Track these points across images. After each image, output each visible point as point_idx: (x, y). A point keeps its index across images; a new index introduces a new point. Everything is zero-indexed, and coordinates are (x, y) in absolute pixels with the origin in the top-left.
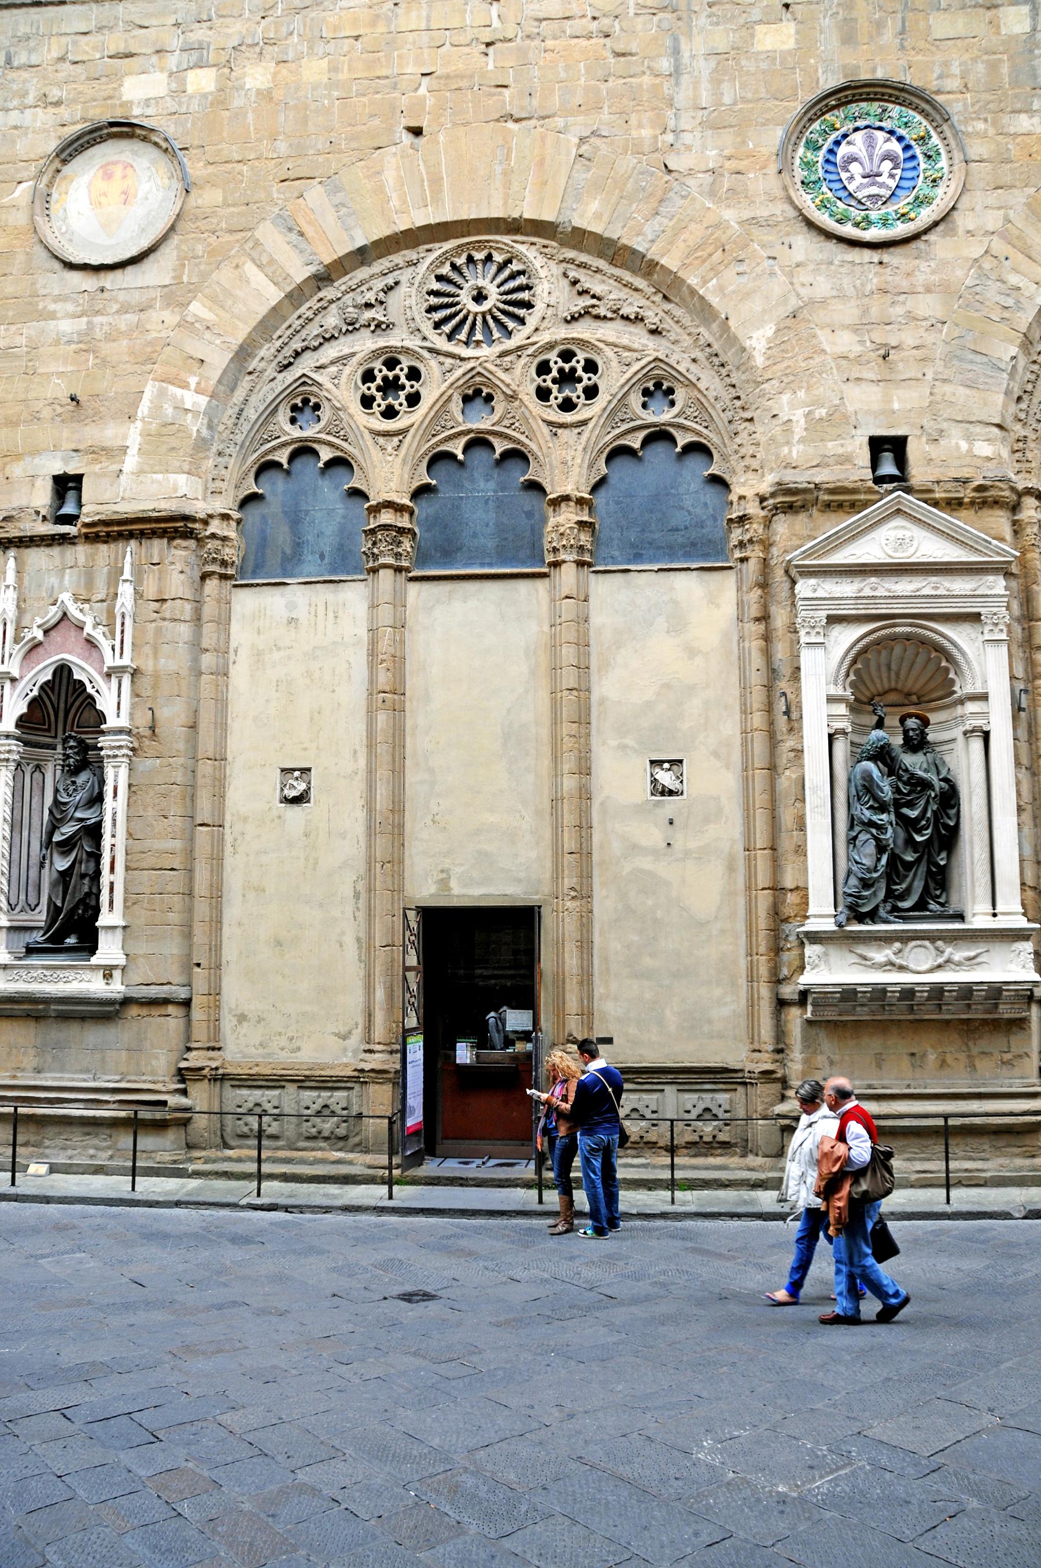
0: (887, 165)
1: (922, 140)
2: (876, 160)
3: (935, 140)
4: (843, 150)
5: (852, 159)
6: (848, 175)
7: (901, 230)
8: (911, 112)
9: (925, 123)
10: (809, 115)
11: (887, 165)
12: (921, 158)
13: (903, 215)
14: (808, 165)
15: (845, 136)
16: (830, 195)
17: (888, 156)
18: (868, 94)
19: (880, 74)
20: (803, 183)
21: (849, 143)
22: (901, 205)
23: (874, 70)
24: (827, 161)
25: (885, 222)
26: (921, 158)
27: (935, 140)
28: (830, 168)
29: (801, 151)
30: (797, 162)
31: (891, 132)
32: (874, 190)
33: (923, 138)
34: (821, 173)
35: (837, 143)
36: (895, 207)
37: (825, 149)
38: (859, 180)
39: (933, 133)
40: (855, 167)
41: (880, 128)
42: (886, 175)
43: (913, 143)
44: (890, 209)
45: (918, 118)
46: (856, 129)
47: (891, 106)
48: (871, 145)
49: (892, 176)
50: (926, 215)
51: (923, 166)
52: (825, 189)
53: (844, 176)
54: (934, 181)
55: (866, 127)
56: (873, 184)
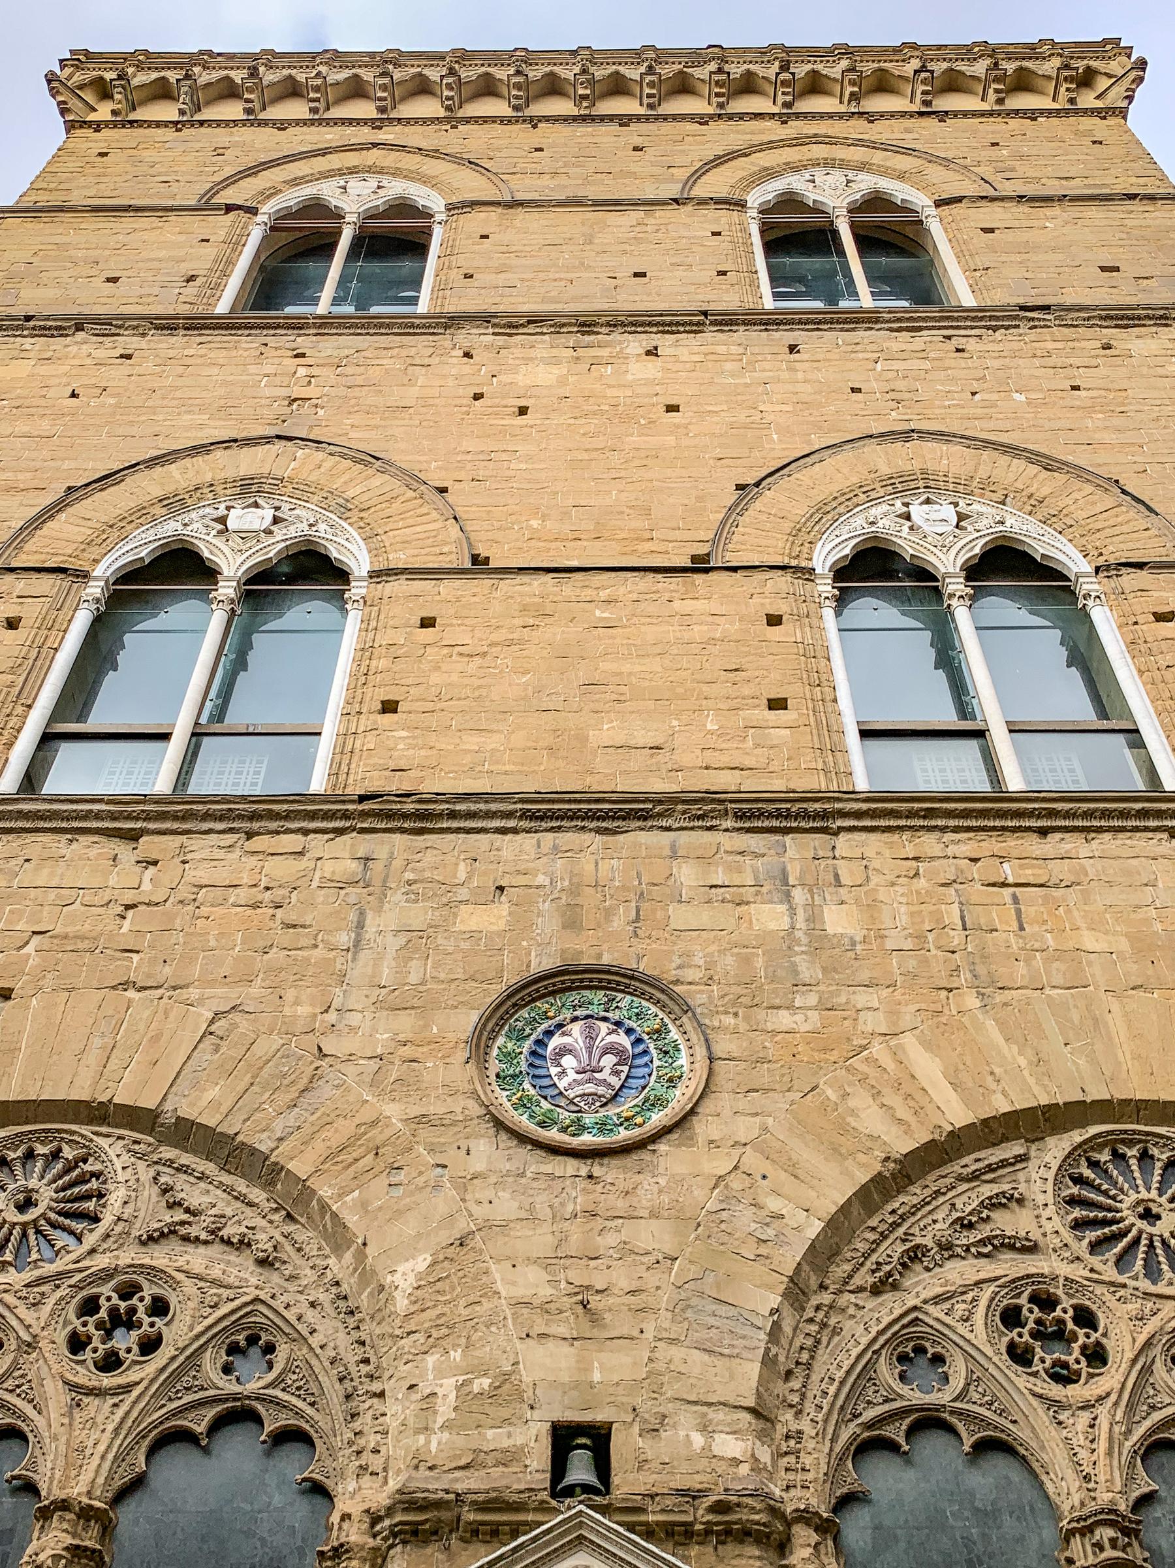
0: (609, 1060)
1: (659, 1033)
2: (596, 1053)
3: (674, 1034)
4: (555, 1042)
5: (563, 1051)
6: (559, 1069)
7: (623, 1135)
8: (644, 1003)
9: (661, 1015)
10: (514, 1000)
11: (609, 1060)
12: (654, 1052)
13: (627, 1119)
14: (509, 1057)
15: (560, 1026)
16: (532, 1092)
17: (610, 1049)
18: (591, 980)
19: (606, 960)
20: (498, 1076)
21: (564, 1034)
22: (625, 1107)
23: (600, 956)
24: (533, 1053)
25: (602, 1127)
26: (654, 1052)
27: (674, 1034)
28: (538, 1062)
29: (501, 1041)
30: (495, 1052)
31: (618, 1024)
32: (590, 1088)
33: (658, 1031)
34: (524, 1067)
35: (549, 1033)
36: (618, 1110)
37: (533, 1038)
38: (572, 1076)
39: (670, 1026)
40: (568, 1061)
41: (605, 1019)
42: (607, 1071)
43: (646, 1037)
44: (612, 1111)
45: (654, 1009)
46: (575, 1019)
47: (620, 996)
48: (590, 1037)
49: (616, 1073)
50: (657, 1119)
51: (656, 1063)
52: (526, 1085)
53: (554, 1071)
54: (670, 1080)
55: (587, 1017)
56: (589, 1081)
